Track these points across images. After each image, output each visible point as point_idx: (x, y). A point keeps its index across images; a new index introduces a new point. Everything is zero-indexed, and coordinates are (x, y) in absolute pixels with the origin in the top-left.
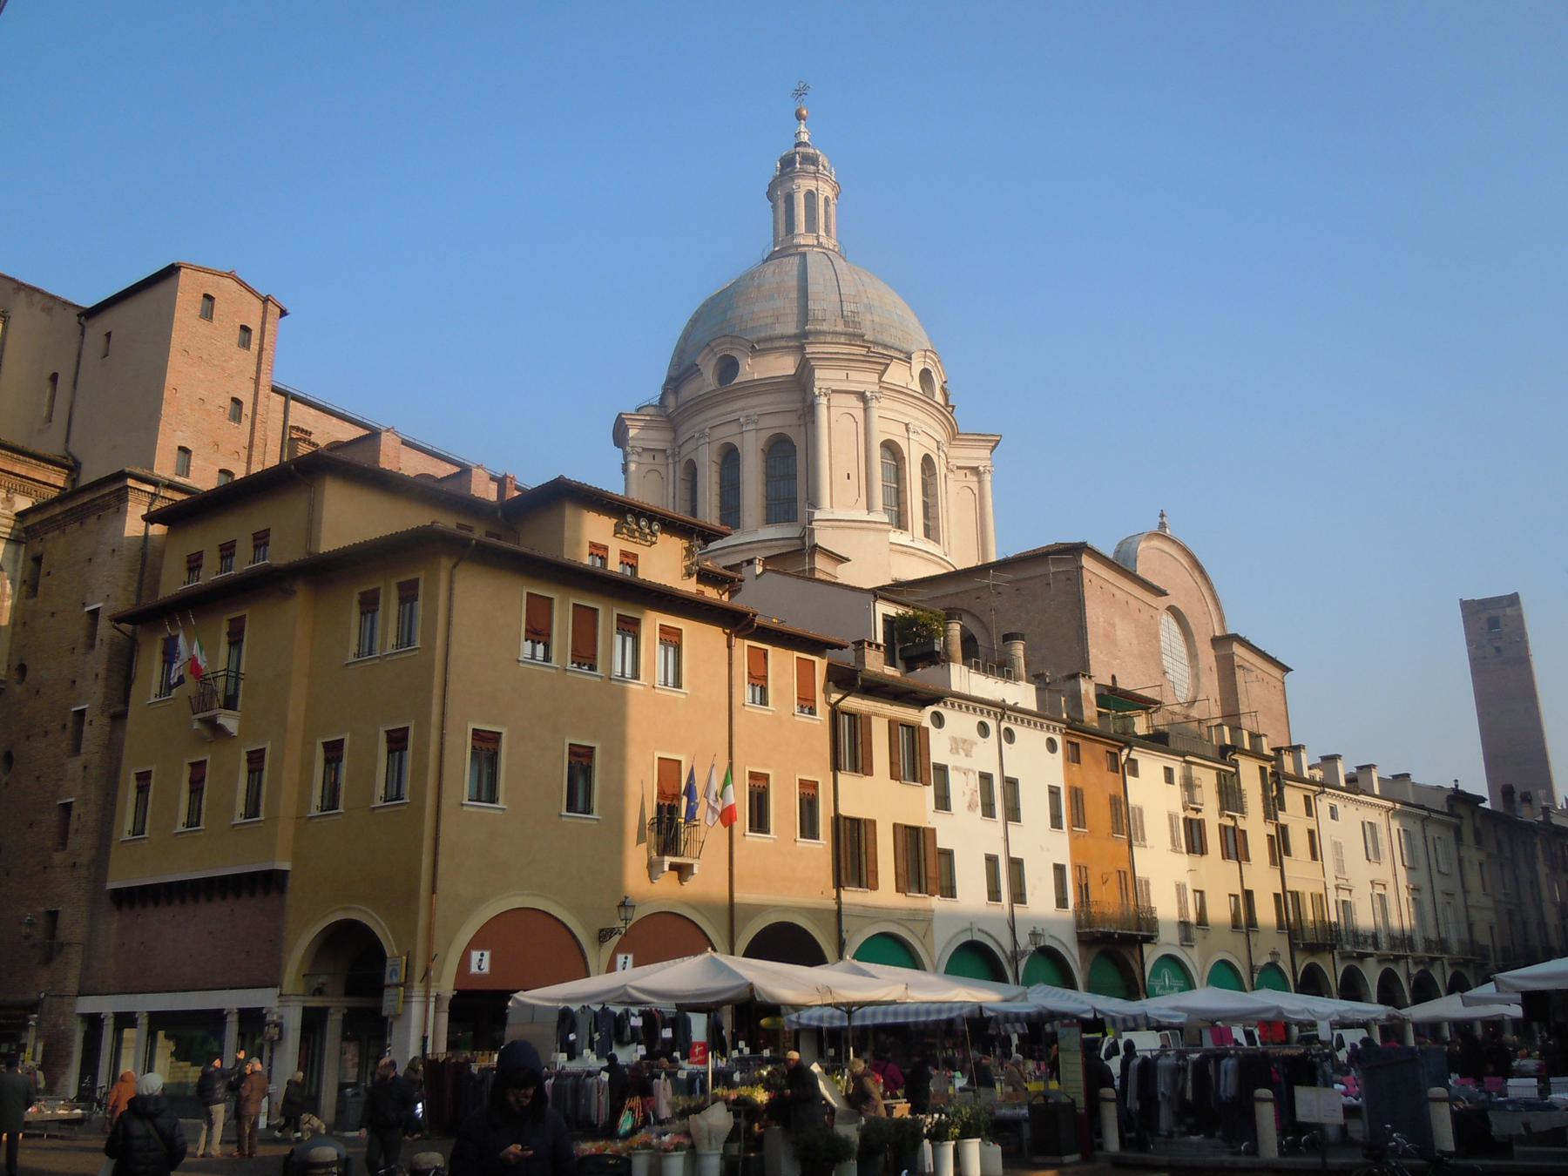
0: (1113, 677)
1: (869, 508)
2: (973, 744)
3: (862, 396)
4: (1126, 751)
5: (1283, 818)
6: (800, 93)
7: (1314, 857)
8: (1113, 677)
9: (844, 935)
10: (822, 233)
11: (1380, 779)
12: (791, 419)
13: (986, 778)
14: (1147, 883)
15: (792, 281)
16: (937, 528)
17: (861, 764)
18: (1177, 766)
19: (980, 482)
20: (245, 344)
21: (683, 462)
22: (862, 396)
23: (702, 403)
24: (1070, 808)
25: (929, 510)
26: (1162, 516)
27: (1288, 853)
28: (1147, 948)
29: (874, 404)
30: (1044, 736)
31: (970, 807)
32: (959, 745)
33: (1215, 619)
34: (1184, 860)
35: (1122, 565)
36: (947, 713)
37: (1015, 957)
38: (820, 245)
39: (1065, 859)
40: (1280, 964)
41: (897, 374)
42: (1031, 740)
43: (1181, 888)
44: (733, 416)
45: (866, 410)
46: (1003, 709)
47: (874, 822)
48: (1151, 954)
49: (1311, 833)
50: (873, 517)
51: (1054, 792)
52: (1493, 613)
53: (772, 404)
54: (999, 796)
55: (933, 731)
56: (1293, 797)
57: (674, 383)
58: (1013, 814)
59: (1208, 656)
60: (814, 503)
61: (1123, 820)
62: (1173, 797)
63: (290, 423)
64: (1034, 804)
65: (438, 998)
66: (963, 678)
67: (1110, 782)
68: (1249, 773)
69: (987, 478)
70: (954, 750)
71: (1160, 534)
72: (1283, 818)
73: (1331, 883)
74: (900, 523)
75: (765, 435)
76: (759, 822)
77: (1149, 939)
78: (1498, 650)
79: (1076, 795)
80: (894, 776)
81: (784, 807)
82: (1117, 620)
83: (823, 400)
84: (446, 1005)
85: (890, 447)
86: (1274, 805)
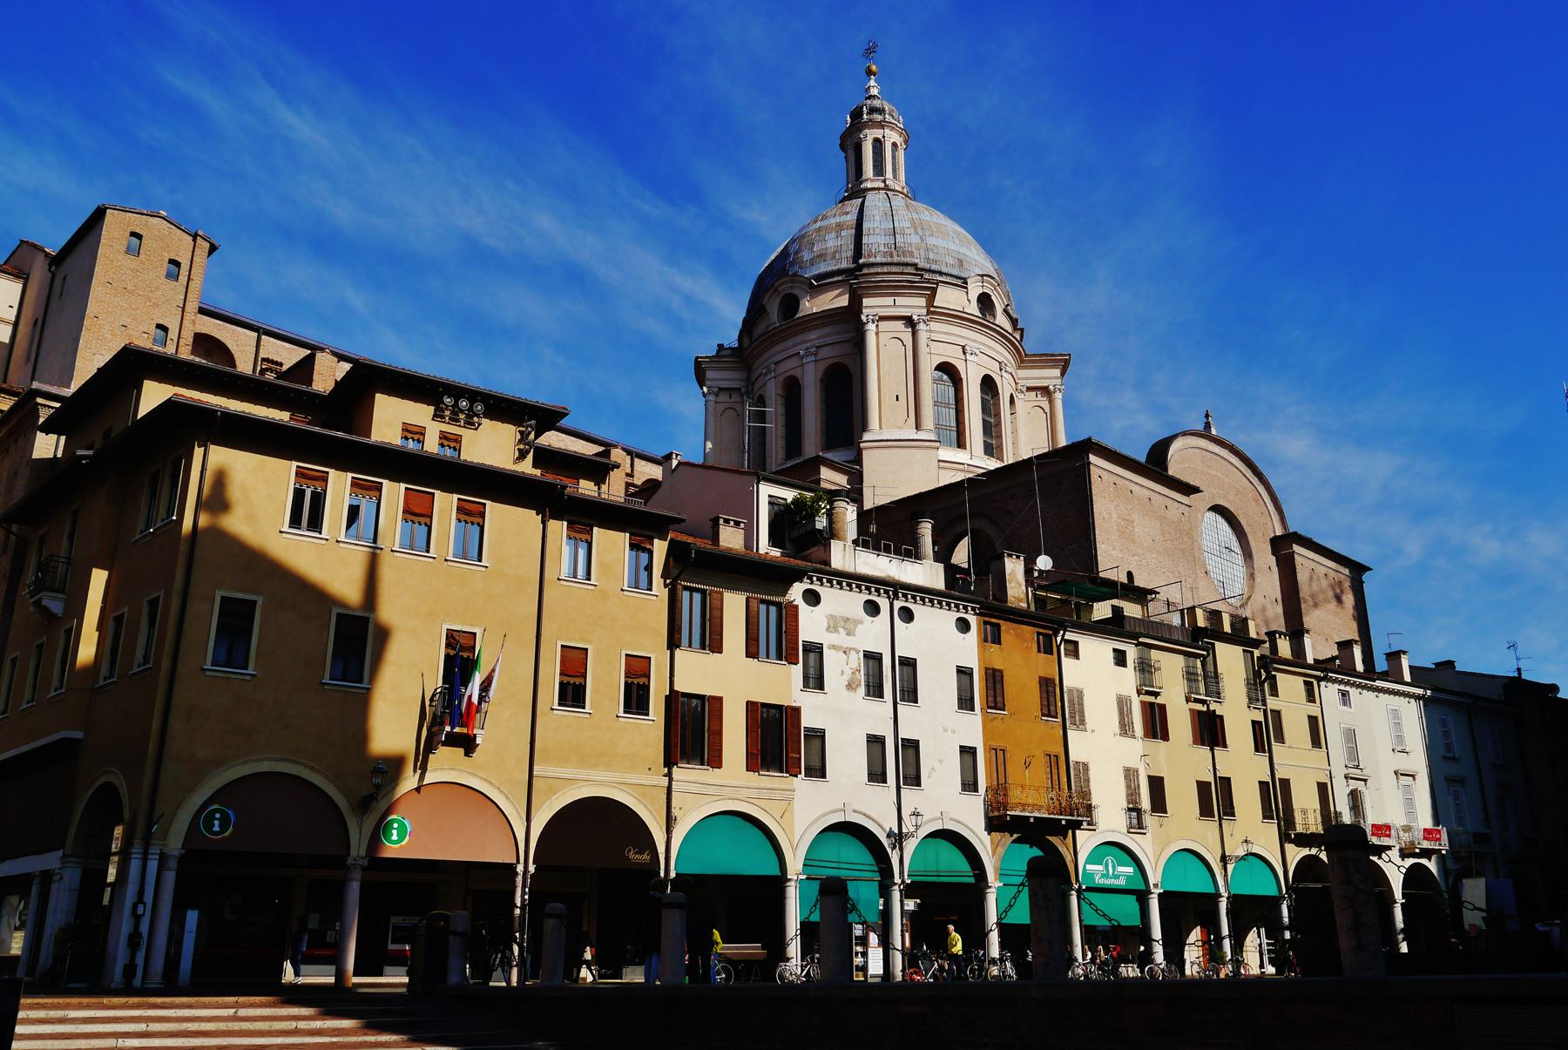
0: (1130, 574)
1: (918, 427)
2: (858, 622)
3: (909, 322)
5: (1272, 703)
6: (870, 51)
8: (1130, 574)
9: (675, 812)
10: (889, 174)
11: (1411, 667)
13: (873, 658)
15: (851, 218)
16: (1000, 447)
17: (712, 641)
18: (1132, 653)
19: (1051, 402)
20: (173, 276)
22: (909, 322)
24: (985, 690)
26: (1207, 416)
27: (1280, 738)
29: (921, 326)
31: (850, 686)
33: (1276, 518)
35: (1154, 465)
36: (824, 591)
37: (899, 838)
38: (887, 188)
39: (976, 740)
41: (947, 297)
43: (1130, 774)
45: (914, 334)
46: (895, 588)
47: (720, 700)
48: (1086, 841)
49: (1313, 721)
50: (921, 435)
51: (964, 673)
53: (829, 335)
54: (893, 678)
56: (1290, 684)
58: (910, 693)
59: (1265, 559)
60: (864, 427)
61: (1054, 700)
62: (1128, 679)
63: (262, 355)
64: (937, 685)
65: (163, 859)
67: (1042, 665)
68: (1231, 660)
69: (1058, 396)
70: (832, 627)
71: (1205, 434)
73: (1339, 771)
74: (961, 444)
75: (823, 366)
76: (573, 694)
77: (1077, 825)
79: (994, 678)
80: (752, 652)
81: (606, 683)
82: (1135, 517)
83: (871, 327)
84: (173, 864)
85: (946, 368)
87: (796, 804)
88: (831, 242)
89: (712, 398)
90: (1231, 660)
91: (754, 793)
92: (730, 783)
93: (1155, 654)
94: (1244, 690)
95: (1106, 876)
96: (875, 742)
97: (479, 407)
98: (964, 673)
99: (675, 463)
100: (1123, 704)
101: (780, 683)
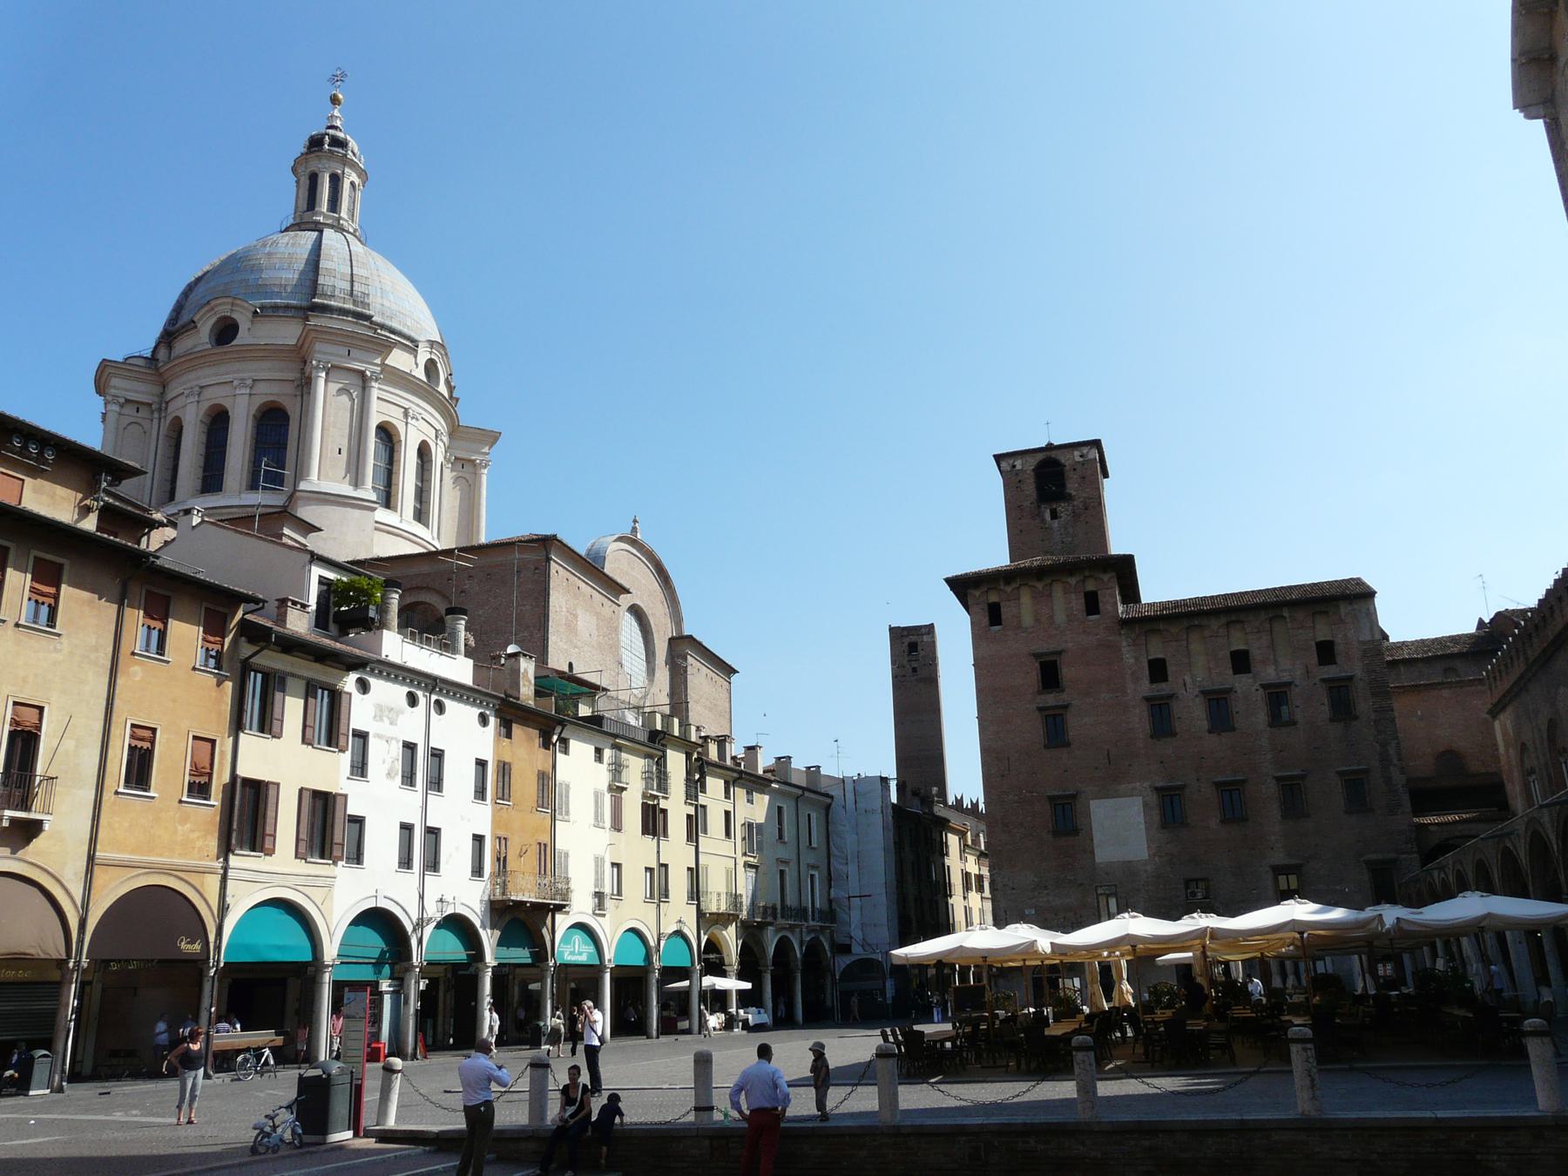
0: (571, 665)
2: (400, 712)
4: (558, 729)
5: (702, 800)
6: (336, 79)
7: (728, 834)
8: (571, 665)
9: (229, 900)
10: (344, 214)
12: (289, 389)
13: (410, 747)
14: (567, 855)
17: (268, 724)
21: (169, 419)
23: (195, 360)
24: (493, 781)
25: (422, 494)
26: (635, 521)
27: (705, 832)
28: (558, 917)
30: (476, 711)
32: (381, 712)
34: (606, 835)
36: (374, 682)
37: (420, 924)
39: (486, 830)
40: (686, 930)
41: (399, 359)
42: (461, 715)
43: (599, 861)
44: (228, 378)
45: (364, 388)
46: (433, 683)
48: (562, 922)
49: (727, 813)
52: (913, 638)
54: (424, 767)
55: (358, 701)
56: (715, 785)
57: (169, 337)
58: (436, 783)
60: (301, 472)
64: (458, 774)
66: (394, 646)
67: (540, 757)
68: (676, 762)
70: (378, 717)
72: (702, 800)
75: (258, 401)
77: (559, 908)
78: (914, 670)
79: (504, 769)
80: (305, 741)
82: (579, 612)
86: (695, 787)
87: (336, 891)
88: (284, 275)
89: (116, 408)
90: (676, 762)
91: (301, 881)
92: (277, 869)
93: (624, 755)
94: (683, 788)
95: (572, 953)
96: (407, 828)
97: (49, 456)
98: (481, 764)
99: (196, 520)
100: (597, 796)
101: (328, 770)
